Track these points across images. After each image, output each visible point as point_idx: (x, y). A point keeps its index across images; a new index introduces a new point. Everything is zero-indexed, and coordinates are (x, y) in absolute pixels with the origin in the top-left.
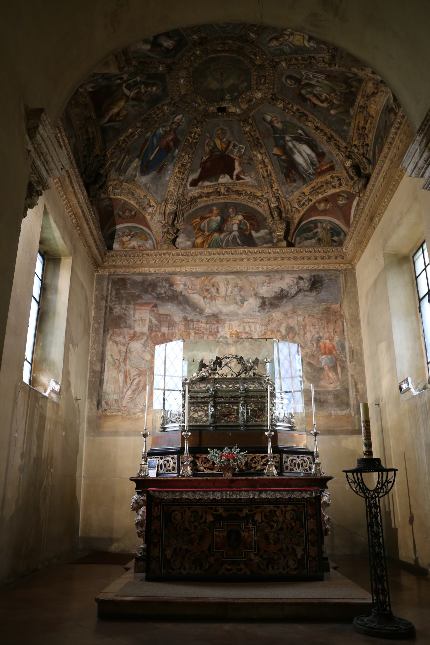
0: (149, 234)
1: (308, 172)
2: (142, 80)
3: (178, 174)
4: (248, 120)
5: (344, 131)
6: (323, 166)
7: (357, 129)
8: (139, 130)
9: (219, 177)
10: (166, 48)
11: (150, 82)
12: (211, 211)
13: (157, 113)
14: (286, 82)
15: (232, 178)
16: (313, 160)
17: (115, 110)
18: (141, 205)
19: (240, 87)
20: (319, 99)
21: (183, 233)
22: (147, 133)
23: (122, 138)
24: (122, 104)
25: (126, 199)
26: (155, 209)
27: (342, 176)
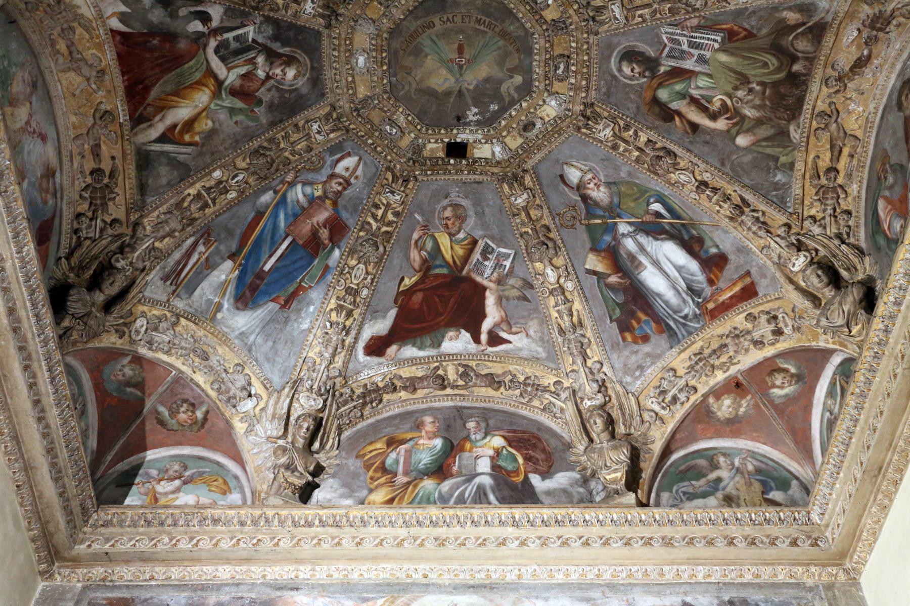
0: (236, 477)
1: (682, 314)
2: (260, 40)
3: (334, 314)
4: (523, 178)
5: (776, 186)
6: (722, 291)
7: (811, 178)
8: (240, 177)
9: (443, 337)
11: (281, 51)
12: (419, 426)
13: (292, 140)
14: (620, 70)
15: (477, 339)
16: (693, 281)
17: (182, 113)
18: (223, 387)
19: (504, 88)
20: (704, 109)
21: (333, 476)
22: (264, 191)
23: (192, 191)
24: (202, 97)
25: (184, 368)
26: (262, 404)
27: (779, 308)
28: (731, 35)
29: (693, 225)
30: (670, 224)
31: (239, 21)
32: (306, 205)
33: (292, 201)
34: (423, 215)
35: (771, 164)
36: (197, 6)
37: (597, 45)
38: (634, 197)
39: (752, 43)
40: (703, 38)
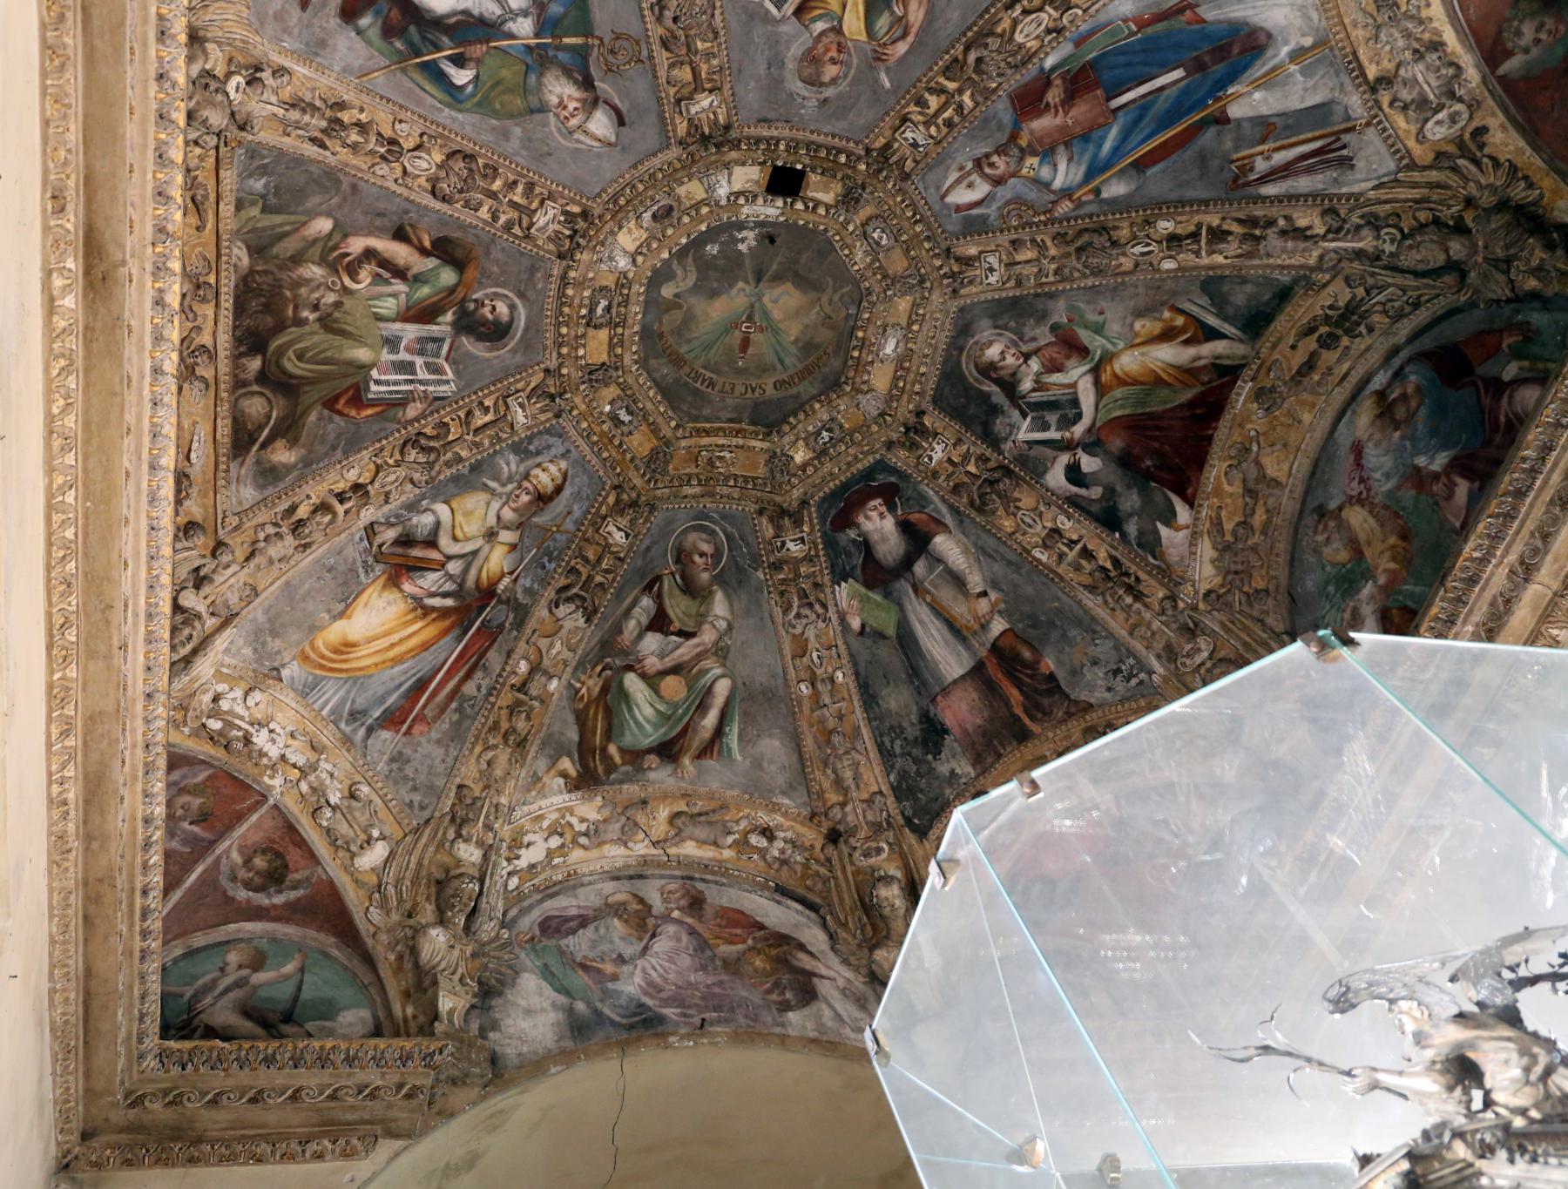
2: (1016, 414)
5: (264, 171)
7: (206, 197)
8: (1139, 249)
10: (891, 507)
11: (995, 388)
14: (512, 307)
17: (1168, 354)
20: (385, 263)
22: (1116, 205)
24: (1128, 362)
28: (358, 398)
29: (401, 58)
30: (439, 49)
31: (1032, 453)
32: (1061, 149)
33: (1079, 164)
34: (876, 81)
35: (273, 200)
36: (1077, 495)
37: (545, 348)
38: (501, 88)
39: (326, 390)
40: (396, 383)
